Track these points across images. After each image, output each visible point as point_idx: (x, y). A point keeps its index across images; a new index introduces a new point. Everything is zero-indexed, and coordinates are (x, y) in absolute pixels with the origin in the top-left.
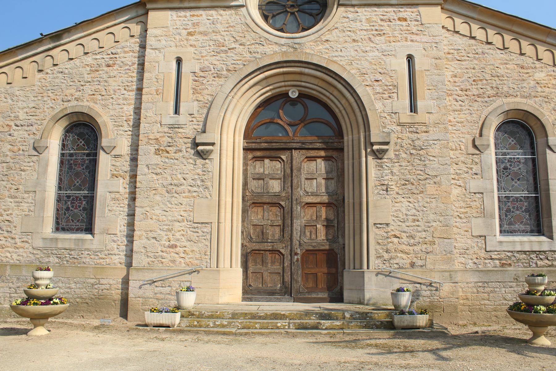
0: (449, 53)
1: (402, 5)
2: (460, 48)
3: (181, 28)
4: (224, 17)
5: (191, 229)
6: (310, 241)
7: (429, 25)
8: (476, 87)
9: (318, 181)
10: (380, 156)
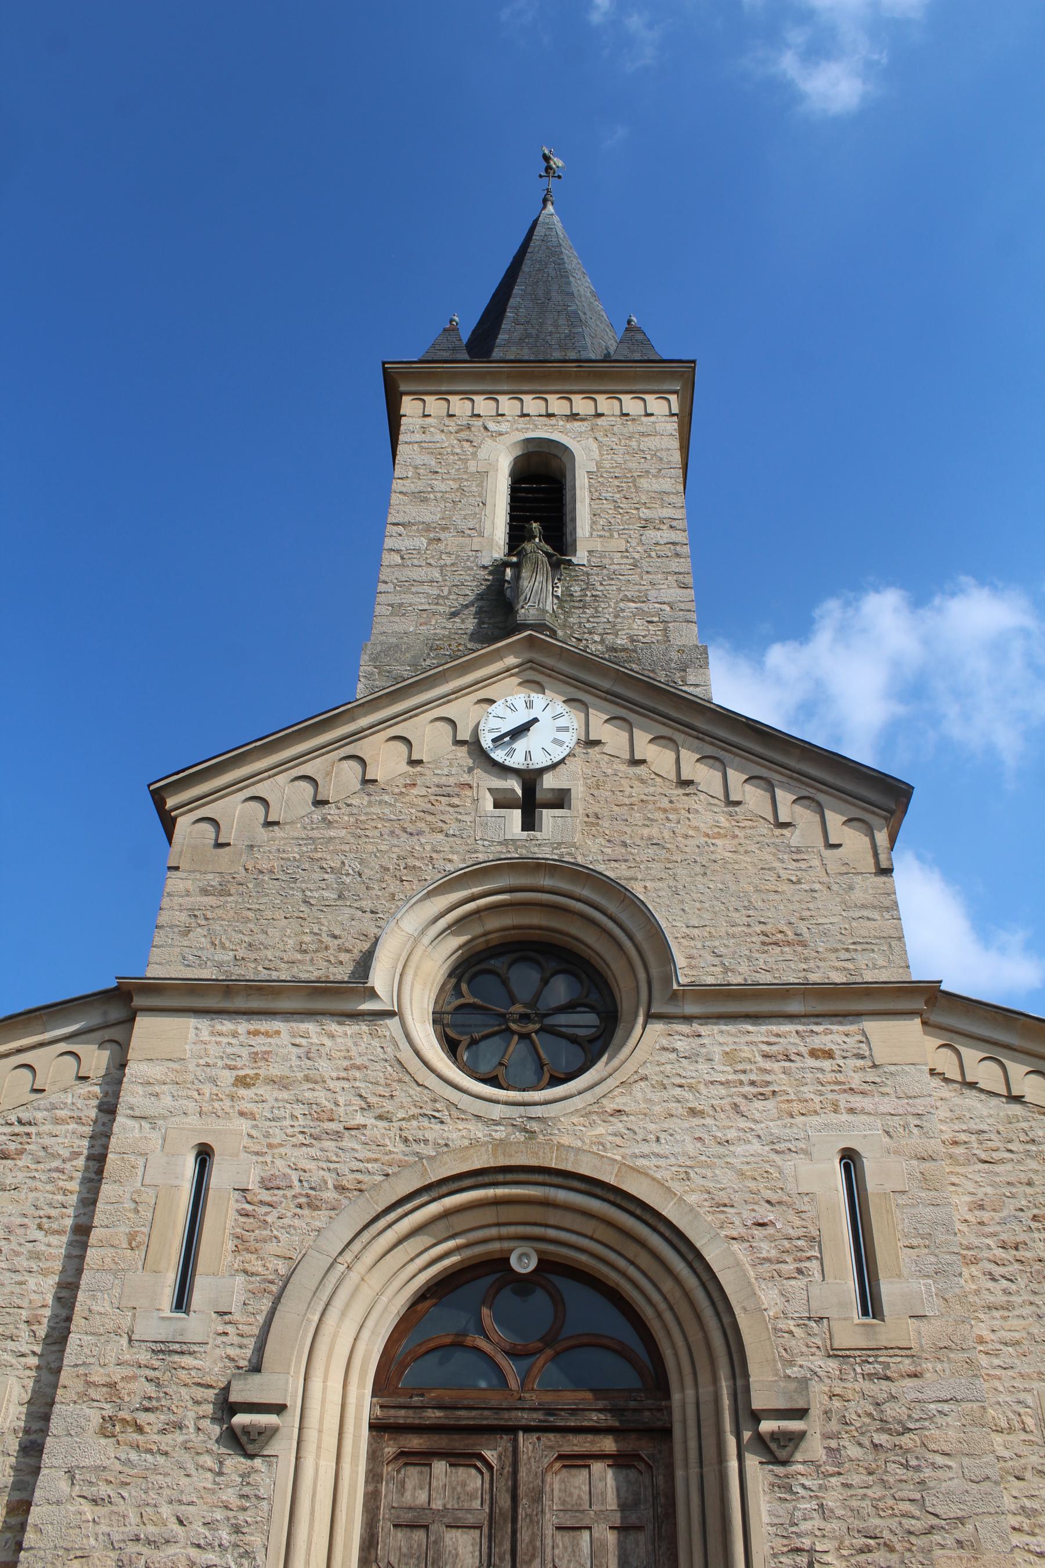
0: (955, 1143)
1: (817, 1016)
2: (985, 1127)
3: (220, 1063)
4: (339, 1040)
7: (893, 1068)
9: (596, 1535)
10: (782, 1454)
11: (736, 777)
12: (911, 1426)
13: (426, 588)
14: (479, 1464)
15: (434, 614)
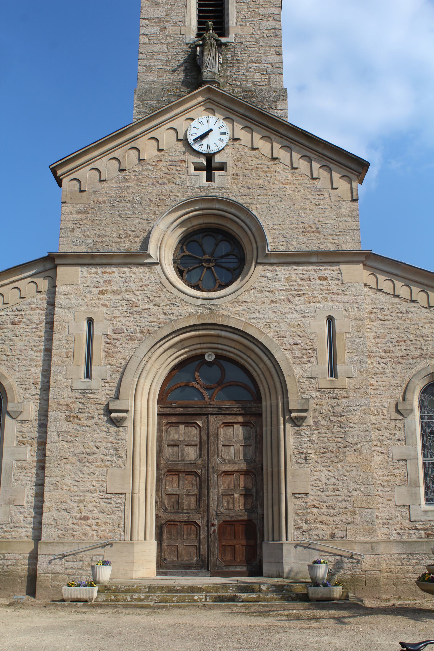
0: (371, 313)
1: (322, 263)
2: (383, 307)
3: (92, 285)
4: (137, 275)
5: (104, 500)
6: (227, 512)
7: (350, 284)
8: (399, 348)
9: (236, 447)
10: (298, 423)
11: (296, 156)
12: (343, 414)
13: (160, 56)
14: (196, 426)
15: (165, 71)
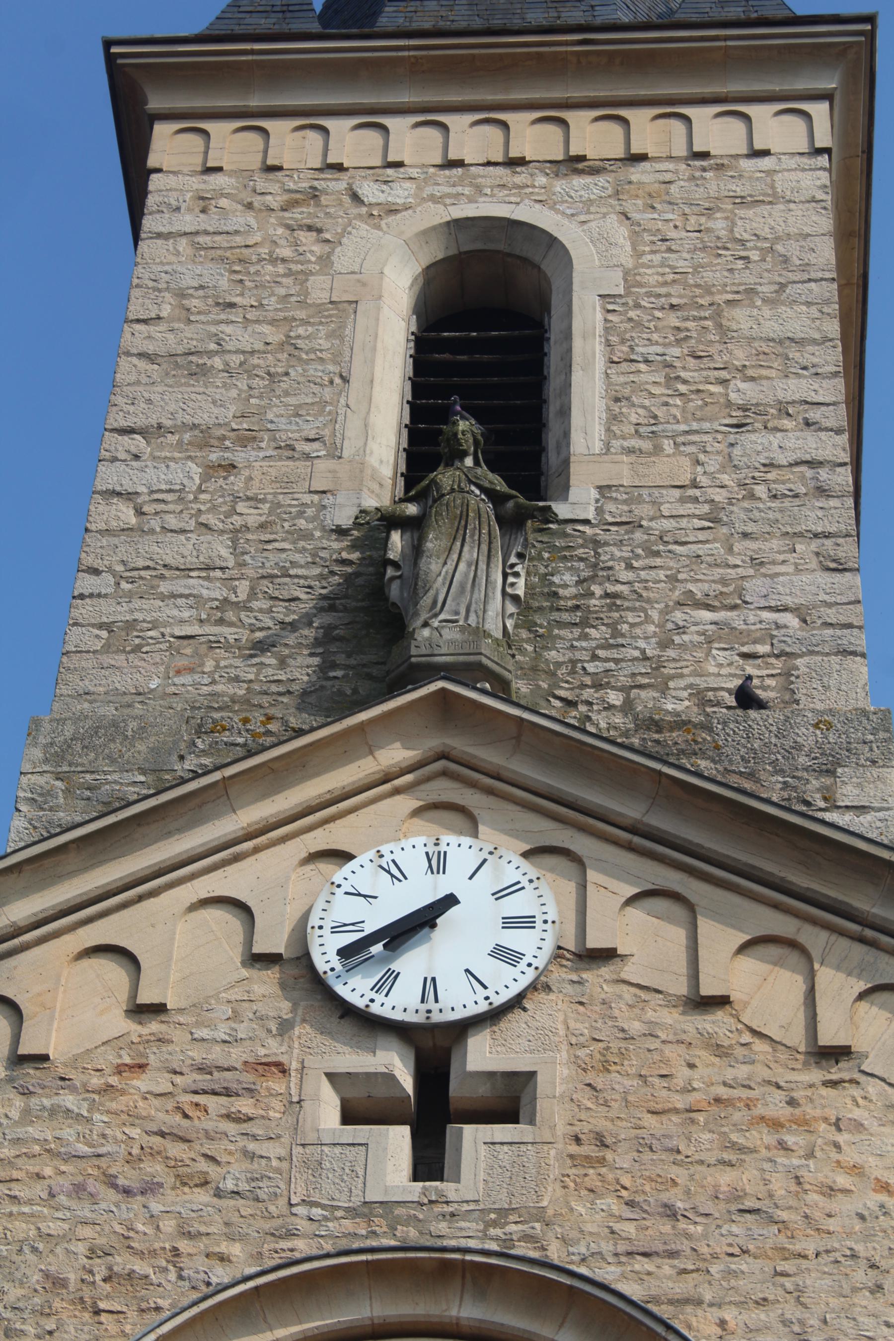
13: (195, 584)
15: (212, 645)
